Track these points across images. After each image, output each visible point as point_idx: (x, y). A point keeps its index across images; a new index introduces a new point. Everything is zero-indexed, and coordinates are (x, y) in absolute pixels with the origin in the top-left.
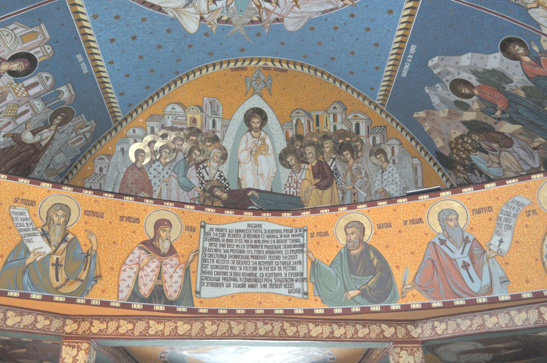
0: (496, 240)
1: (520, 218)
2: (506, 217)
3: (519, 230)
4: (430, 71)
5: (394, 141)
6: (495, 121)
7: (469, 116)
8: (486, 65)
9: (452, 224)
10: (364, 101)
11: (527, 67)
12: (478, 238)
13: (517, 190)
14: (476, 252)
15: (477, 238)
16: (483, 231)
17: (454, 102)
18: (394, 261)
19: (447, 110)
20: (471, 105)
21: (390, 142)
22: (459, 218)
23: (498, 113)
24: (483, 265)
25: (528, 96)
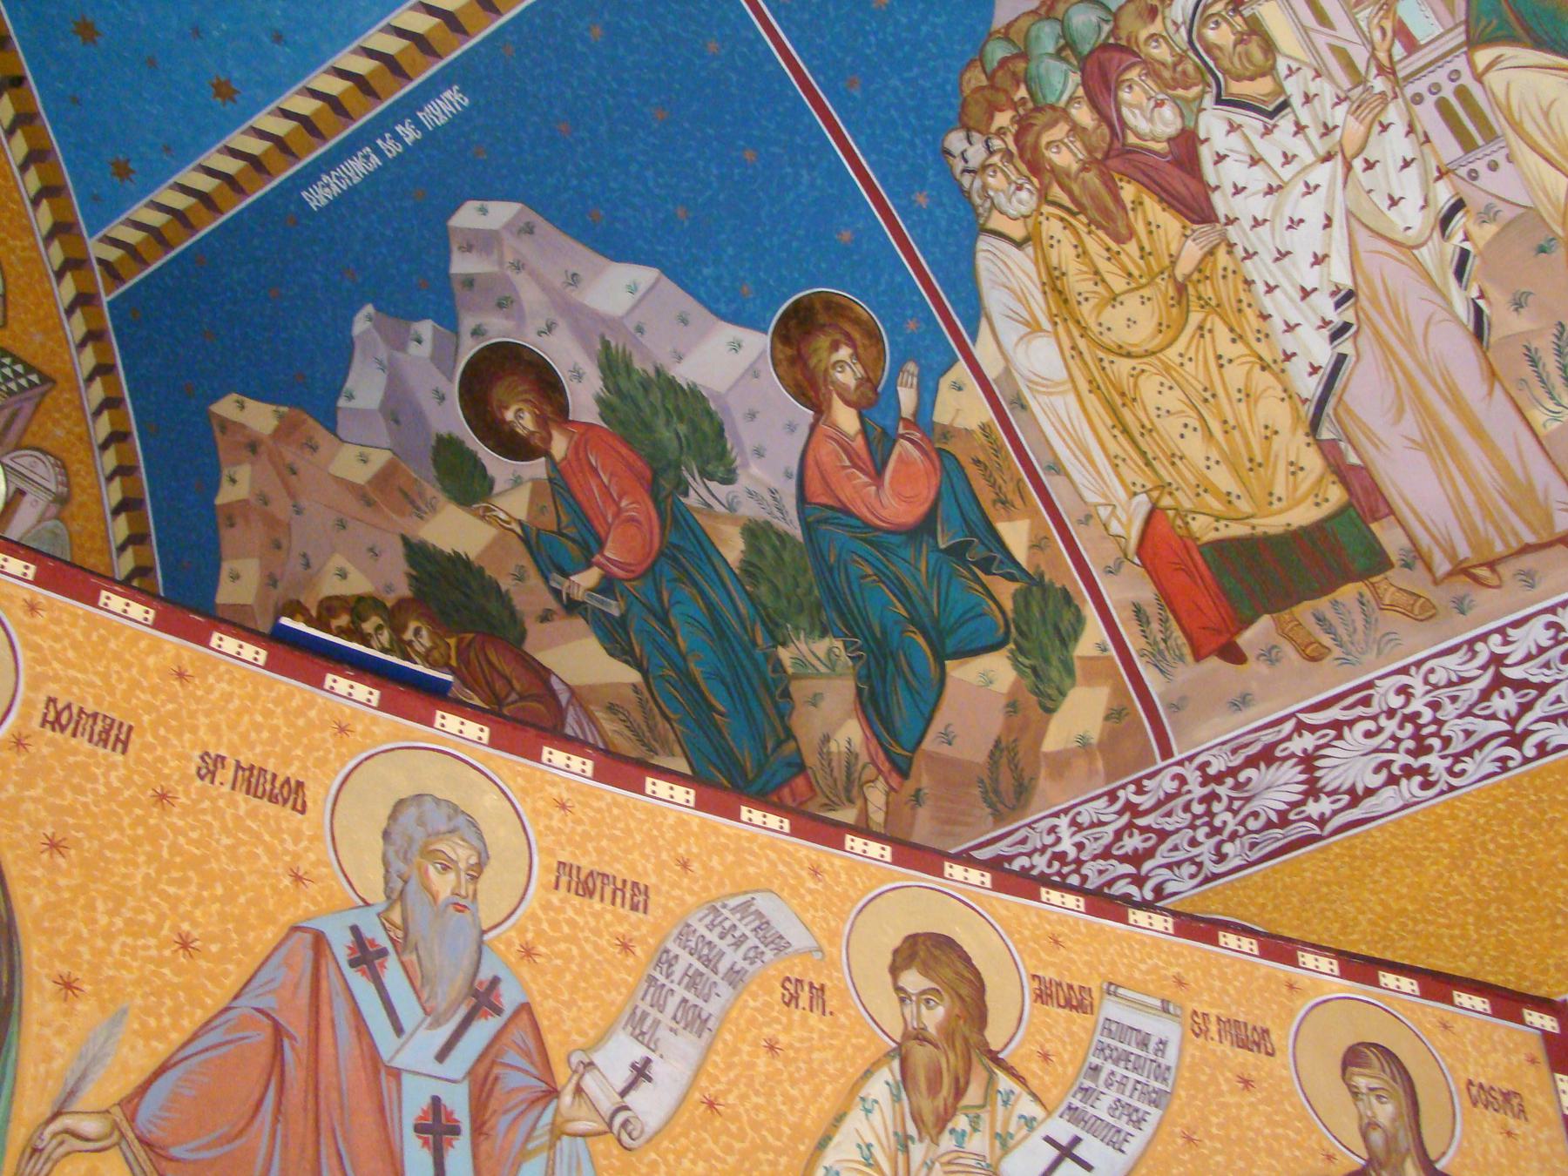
0: (619, 1055)
1: (754, 996)
2: (698, 965)
3: (736, 1051)
4: (442, 244)
5: (41, 469)
6: (553, 604)
7: (455, 531)
8: (680, 358)
9: (444, 884)
10: (36, 202)
11: (826, 451)
12: (544, 1009)
13: (773, 864)
14: (513, 1080)
15: (538, 1011)
16: (573, 988)
17: (440, 439)
18: (60, 943)
19: (380, 458)
20: (497, 489)
21: (25, 460)
22: (488, 872)
23: (587, 579)
24: (524, 1155)
25: (750, 569)
